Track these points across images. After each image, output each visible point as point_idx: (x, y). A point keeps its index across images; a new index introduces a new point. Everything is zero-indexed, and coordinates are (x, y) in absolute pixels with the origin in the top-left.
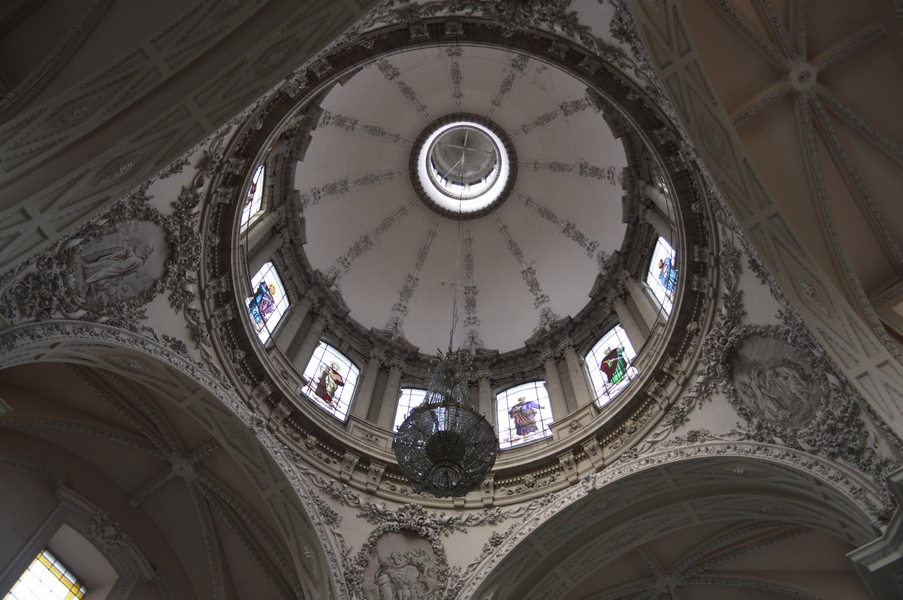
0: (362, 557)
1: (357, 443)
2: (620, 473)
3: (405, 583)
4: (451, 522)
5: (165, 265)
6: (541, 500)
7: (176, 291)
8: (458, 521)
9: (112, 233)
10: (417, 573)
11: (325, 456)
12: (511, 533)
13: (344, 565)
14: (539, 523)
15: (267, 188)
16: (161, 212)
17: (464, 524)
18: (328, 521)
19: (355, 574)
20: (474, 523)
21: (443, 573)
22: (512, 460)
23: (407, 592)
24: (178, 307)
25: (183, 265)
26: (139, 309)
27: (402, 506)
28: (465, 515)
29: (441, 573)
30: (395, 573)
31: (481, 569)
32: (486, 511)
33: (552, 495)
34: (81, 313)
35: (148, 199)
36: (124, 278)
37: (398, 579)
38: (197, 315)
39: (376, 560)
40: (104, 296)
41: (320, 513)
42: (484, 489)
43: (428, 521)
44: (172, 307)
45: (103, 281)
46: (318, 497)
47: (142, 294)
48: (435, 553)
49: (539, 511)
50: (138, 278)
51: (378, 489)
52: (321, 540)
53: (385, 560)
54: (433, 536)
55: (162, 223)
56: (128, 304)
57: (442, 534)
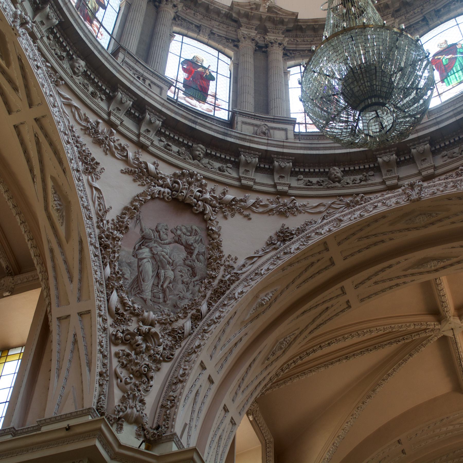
1: (132, 82)
2: (454, 186)
3: (169, 263)
6: (348, 200)
8: (242, 203)
10: (184, 254)
11: (91, 89)
13: (98, 227)
14: (342, 225)
17: (249, 208)
18: (87, 169)
20: (261, 210)
22: (318, 146)
23: (170, 274)
27: (178, 172)
33: (363, 197)
37: (162, 257)
39: (138, 230)
41: (79, 158)
43: (208, 196)
46: (78, 137)
48: (209, 235)
49: (342, 212)
53: (148, 231)
57: (221, 215)
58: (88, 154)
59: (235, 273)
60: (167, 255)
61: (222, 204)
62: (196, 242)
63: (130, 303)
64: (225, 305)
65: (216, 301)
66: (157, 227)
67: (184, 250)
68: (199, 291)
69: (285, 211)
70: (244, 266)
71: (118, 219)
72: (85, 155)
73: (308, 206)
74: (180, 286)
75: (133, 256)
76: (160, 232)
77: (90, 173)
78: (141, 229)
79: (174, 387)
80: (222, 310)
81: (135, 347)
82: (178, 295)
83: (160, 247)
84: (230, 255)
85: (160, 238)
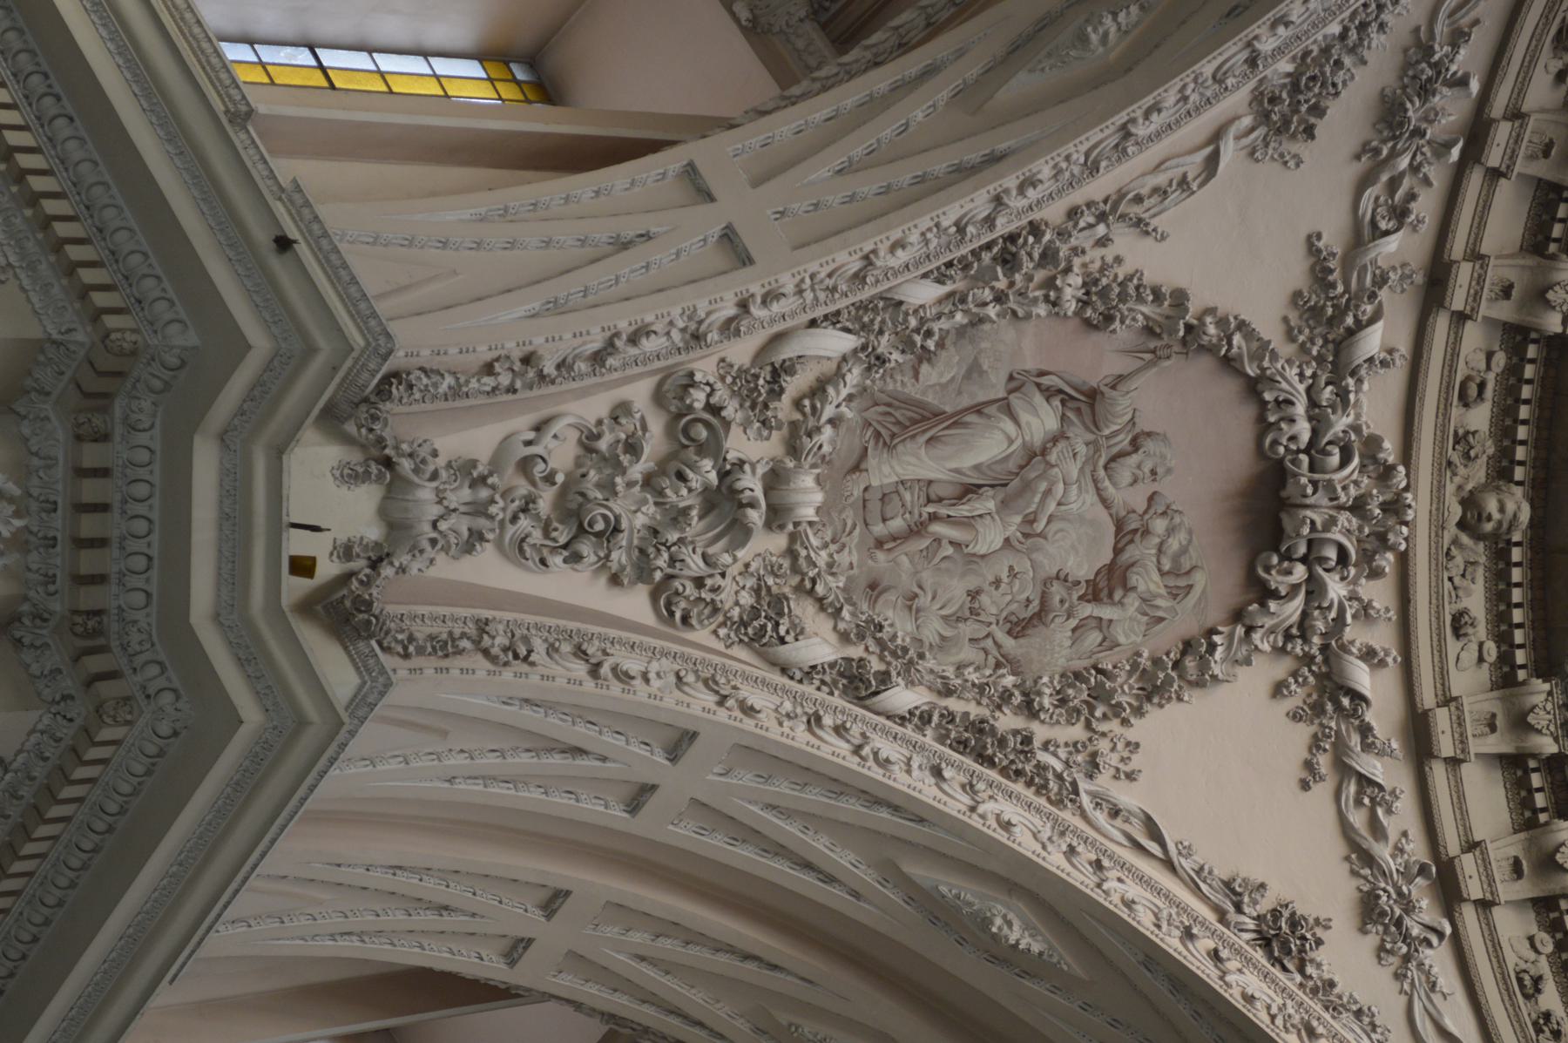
0: (1123, 297)
3: (1030, 520)
4: (1346, 702)
8: (1355, 740)
10: (1083, 568)
12: (1334, 1008)
13: (1073, 213)
17: (1343, 769)
18: (1274, 100)
19: (1040, 275)
20: (1358, 819)
21: (1099, 695)
23: (990, 538)
27: (1390, 450)
28: (1392, 772)
29: (1100, 685)
30: (1068, 465)
31: (1142, 880)
32: (1423, 870)
37: (1043, 486)
39: (1116, 365)
41: (1307, 53)
42: (1527, 850)
43: (1336, 589)
46: (1382, 27)
48: (1188, 646)
51: (1461, 318)
52: (1176, 84)
53: (1122, 405)
54: (1269, 622)
57: (1281, 669)
58: (1334, 85)
59: (1074, 784)
60: (1059, 504)
61: (1326, 661)
62: (1144, 600)
63: (829, 412)
64: (937, 772)
65: (941, 739)
66: (1149, 434)
67: (1099, 565)
68: (960, 668)
69: (1383, 914)
70: (1115, 813)
71: (1130, 278)
72: (1323, 73)
73: (1436, 998)
74: (956, 589)
75: (1011, 378)
76: (1136, 450)
77: (1264, 117)
78: (1120, 378)
79: (566, 648)
80: (915, 765)
81: (673, 469)
82: (920, 587)
83: (1082, 470)
84: (1137, 745)
85: (1113, 459)
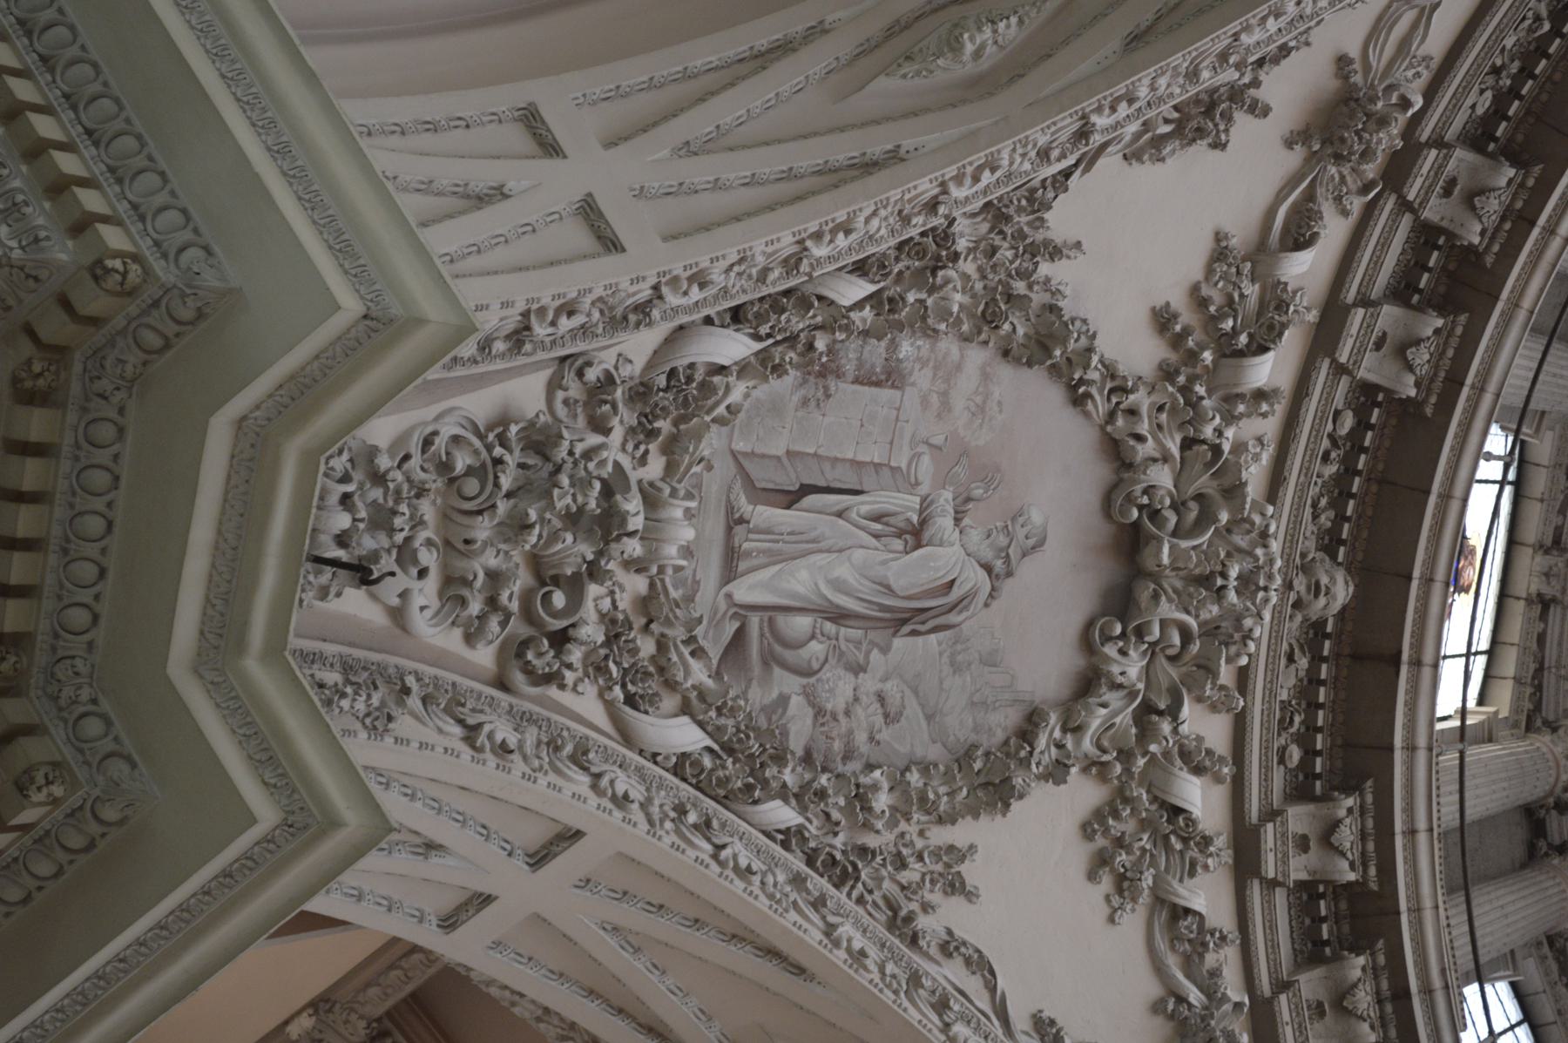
5: (1088, 642)
7: (1121, 796)
9: (878, 384)
15: (1517, 608)
16: (1106, 346)
24: (1124, 884)
25: (1173, 659)
26: (941, 836)
34: (685, 736)
35: (1055, 252)
36: (898, 642)
38: (1210, 959)
40: (796, 702)
44: (1092, 876)
45: (802, 623)
47: (964, 758)
50: (956, 668)
55: (1099, 406)
56: (898, 784)
